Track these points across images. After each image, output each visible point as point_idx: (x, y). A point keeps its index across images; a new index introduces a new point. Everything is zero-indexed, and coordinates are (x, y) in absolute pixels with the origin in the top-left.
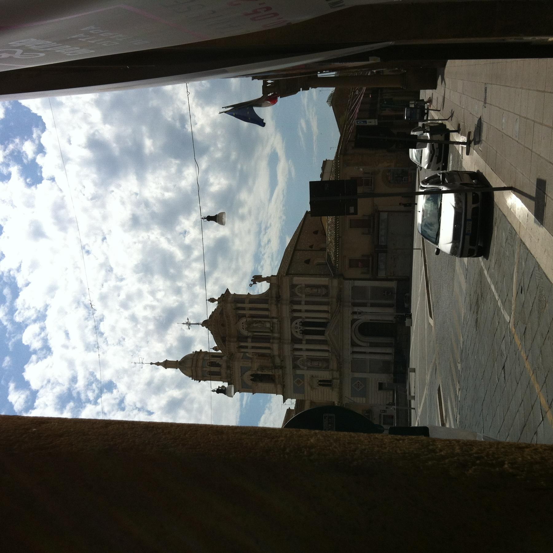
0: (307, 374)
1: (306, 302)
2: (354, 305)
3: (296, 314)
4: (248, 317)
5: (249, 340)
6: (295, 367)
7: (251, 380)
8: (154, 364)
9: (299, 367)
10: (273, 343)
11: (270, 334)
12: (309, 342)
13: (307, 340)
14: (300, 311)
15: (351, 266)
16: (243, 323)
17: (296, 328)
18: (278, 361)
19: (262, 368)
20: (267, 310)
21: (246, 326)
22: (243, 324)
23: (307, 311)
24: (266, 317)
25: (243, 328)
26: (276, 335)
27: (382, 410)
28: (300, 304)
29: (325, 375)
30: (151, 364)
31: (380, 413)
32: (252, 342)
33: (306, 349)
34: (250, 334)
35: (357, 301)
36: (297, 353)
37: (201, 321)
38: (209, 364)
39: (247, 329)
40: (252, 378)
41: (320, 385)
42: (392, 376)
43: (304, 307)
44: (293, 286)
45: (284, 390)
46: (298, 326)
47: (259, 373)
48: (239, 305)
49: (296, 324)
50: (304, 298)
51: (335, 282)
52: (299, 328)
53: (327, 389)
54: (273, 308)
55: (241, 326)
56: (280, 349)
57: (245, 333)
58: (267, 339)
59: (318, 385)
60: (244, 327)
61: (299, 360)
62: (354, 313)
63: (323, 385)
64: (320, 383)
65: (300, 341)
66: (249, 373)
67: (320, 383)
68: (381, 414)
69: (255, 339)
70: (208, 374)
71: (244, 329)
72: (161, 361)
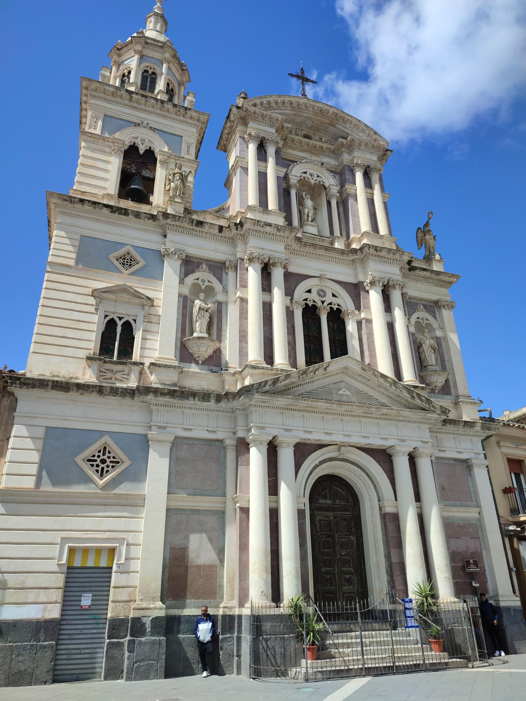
9: (186, 275)
21: (313, 182)
22: (316, 176)
25: (305, 173)
41: (111, 324)
46: (329, 299)
49: (334, 295)
52: (323, 299)
59: (108, 319)
64: (120, 323)
67: (120, 323)
70: (148, 69)
71: (304, 175)
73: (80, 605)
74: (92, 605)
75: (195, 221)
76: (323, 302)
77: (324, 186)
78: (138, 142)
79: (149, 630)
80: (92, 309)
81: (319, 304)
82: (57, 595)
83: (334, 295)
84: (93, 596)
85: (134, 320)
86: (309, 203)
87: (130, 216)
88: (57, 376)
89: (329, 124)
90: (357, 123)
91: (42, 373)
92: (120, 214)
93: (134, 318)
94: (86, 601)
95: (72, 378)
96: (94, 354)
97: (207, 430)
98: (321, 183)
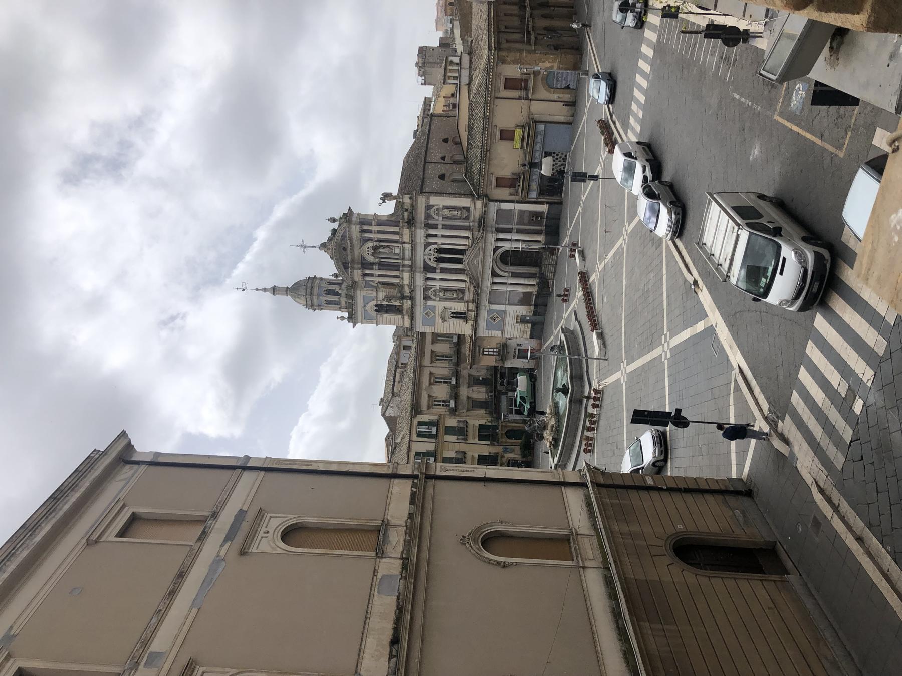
0: (439, 305)
1: (443, 225)
2: (499, 230)
3: (431, 240)
4: (376, 241)
5: (376, 267)
6: (426, 298)
7: (376, 311)
8: (260, 290)
9: (430, 297)
10: (403, 271)
11: (399, 261)
12: (443, 271)
13: (442, 269)
14: (436, 236)
15: (497, 186)
16: (368, 248)
17: (430, 255)
18: (407, 291)
19: (389, 298)
20: (397, 233)
21: (373, 251)
23: (443, 236)
24: (397, 242)
25: (368, 254)
26: (407, 263)
28: (437, 228)
29: (460, 307)
30: (257, 290)
32: (379, 269)
33: (440, 279)
34: (377, 260)
35: (501, 226)
36: (430, 283)
37: (318, 244)
38: (325, 292)
39: (373, 254)
40: (376, 308)
41: (452, 317)
42: (532, 308)
43: (439, 232)
44: (429, 207)
47: (385, 303)
48: (366, 227)
49: (430, 250)
50: (440, 221)
51: (479, 204)
53: (460, 322)
54: (406, 232)
55: (367, 252)
56: (412, 278)
57: (371, 259)
58: (396, 267)
60: (370, 253)
61: (431, 290)
62: (497, 240)
63: (456, 318)
64: (452, 315)
65: (433, 270)
66: (375, 303)
67: (452, 315)
69: (382, 266)
72: (268, 287)
78: (373, 310)
80: (449, 323)
82: (526, 326)
86: (381, 250)
94: (528, 318)
96: (464, 321)
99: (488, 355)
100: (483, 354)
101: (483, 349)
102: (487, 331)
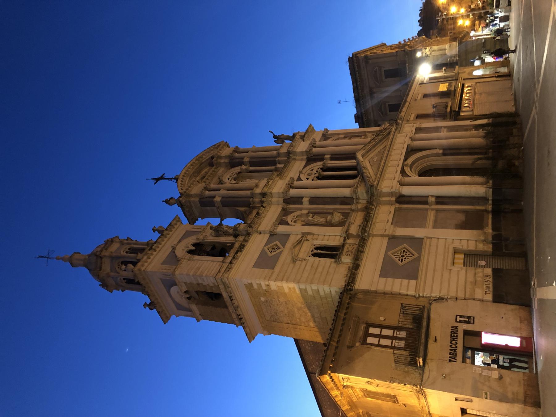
16: (232, 174)
27: (461, 317)
31: (456, 324)
41: (315, 255)
45: (238, 254)
49: (312, 170)
52: (314, 173)
64: (315, 251)
68: (456, 327)
73: (485, 265)
74: (485, 261)
75: (256, 215)
76: (315, 174)
77: (239, 173)
78: (187, 249)
79: (499, 233)
81: (317, 175)
83: (312, 170)
84: (480, 260)
85: (314, 246)
87: (245, 244)
88: (347, 275)
89: (200, 165)
90: (205, 152)
91: (344, 281)
92: (243, 248)
93: (313, 245)
95: (349, 269)
97: (389, 214)
98: (237, 173)
99: (379, 345)
100: (364, 342)
101: (367, 330)
102: (383, 280)
